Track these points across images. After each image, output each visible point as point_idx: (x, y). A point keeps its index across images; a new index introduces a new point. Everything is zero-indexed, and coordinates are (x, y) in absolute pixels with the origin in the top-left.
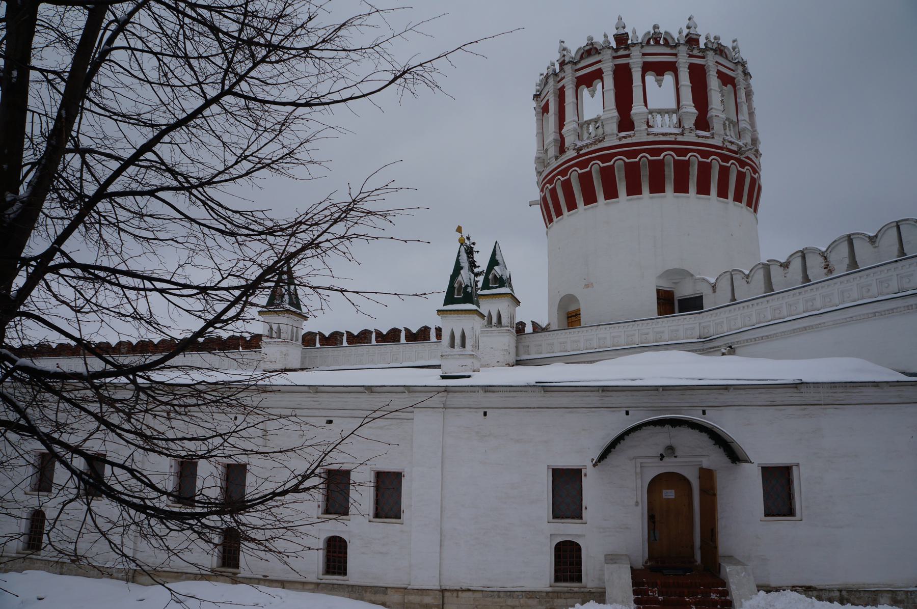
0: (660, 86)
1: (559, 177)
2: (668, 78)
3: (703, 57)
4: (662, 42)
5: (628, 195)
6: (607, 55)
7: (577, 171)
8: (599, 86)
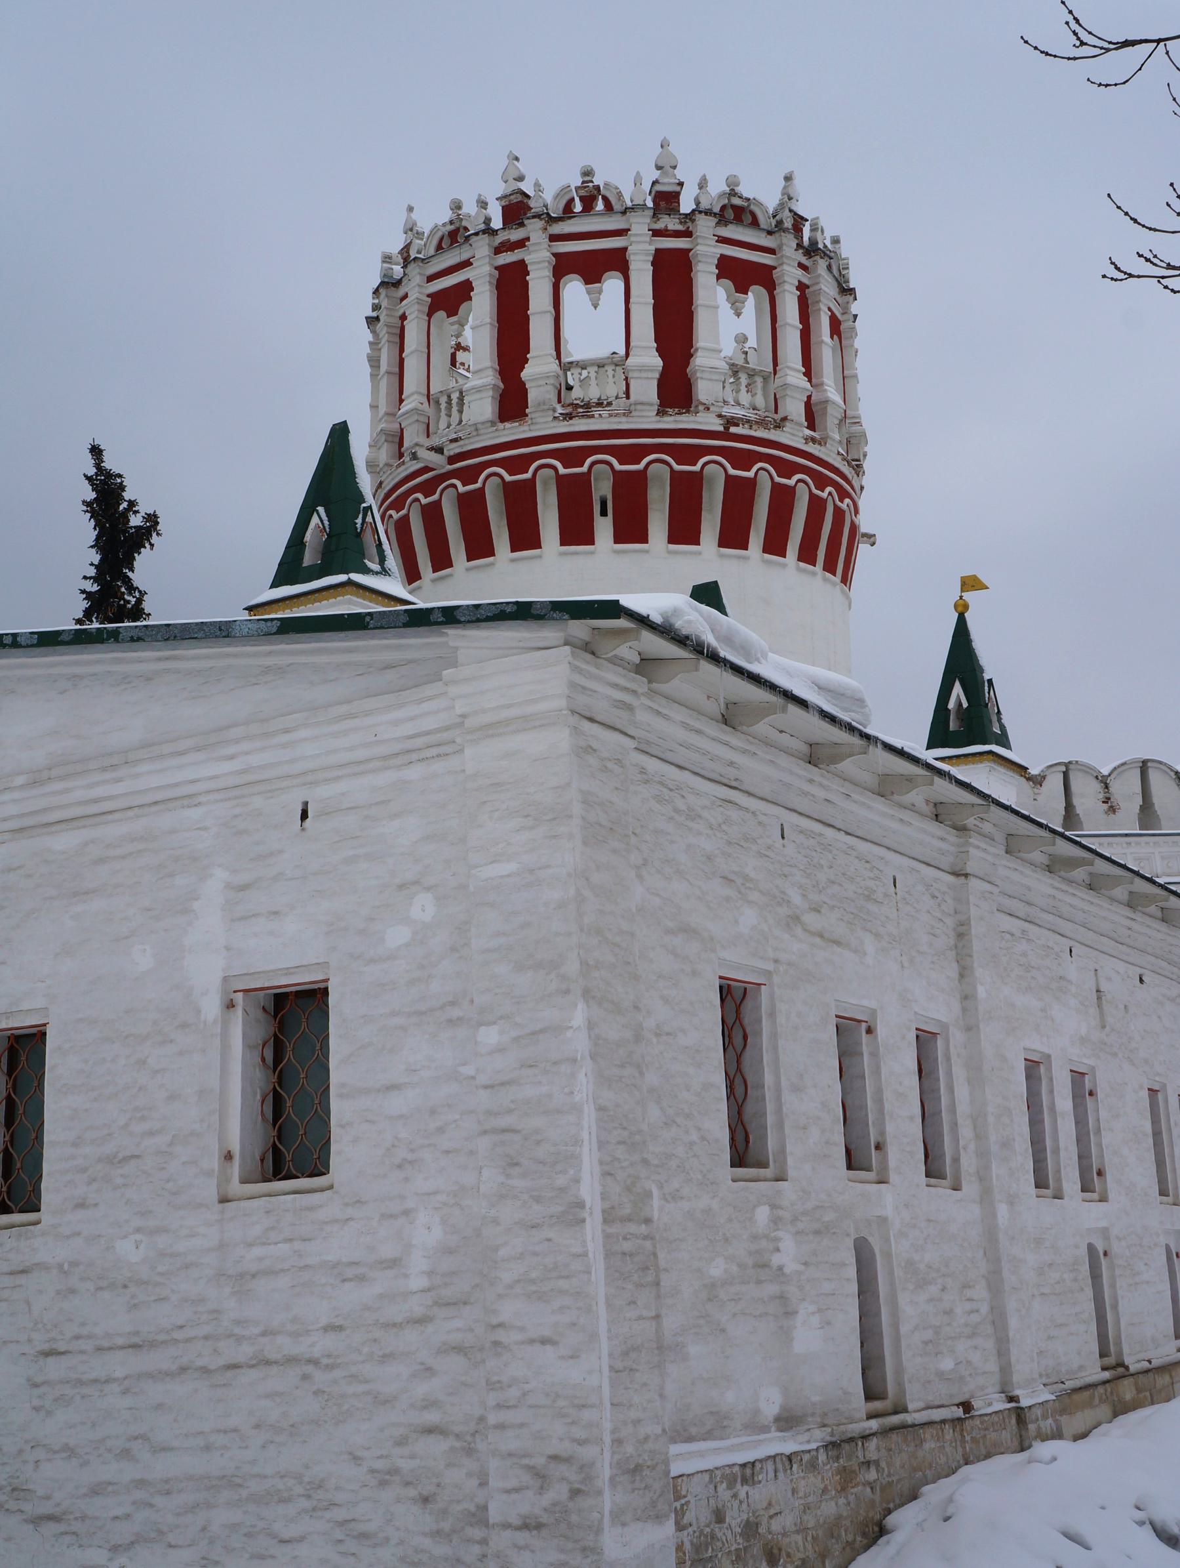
1: (419, 495)
2: (612, 285)
3: (688, 234)
7: (454, 486)
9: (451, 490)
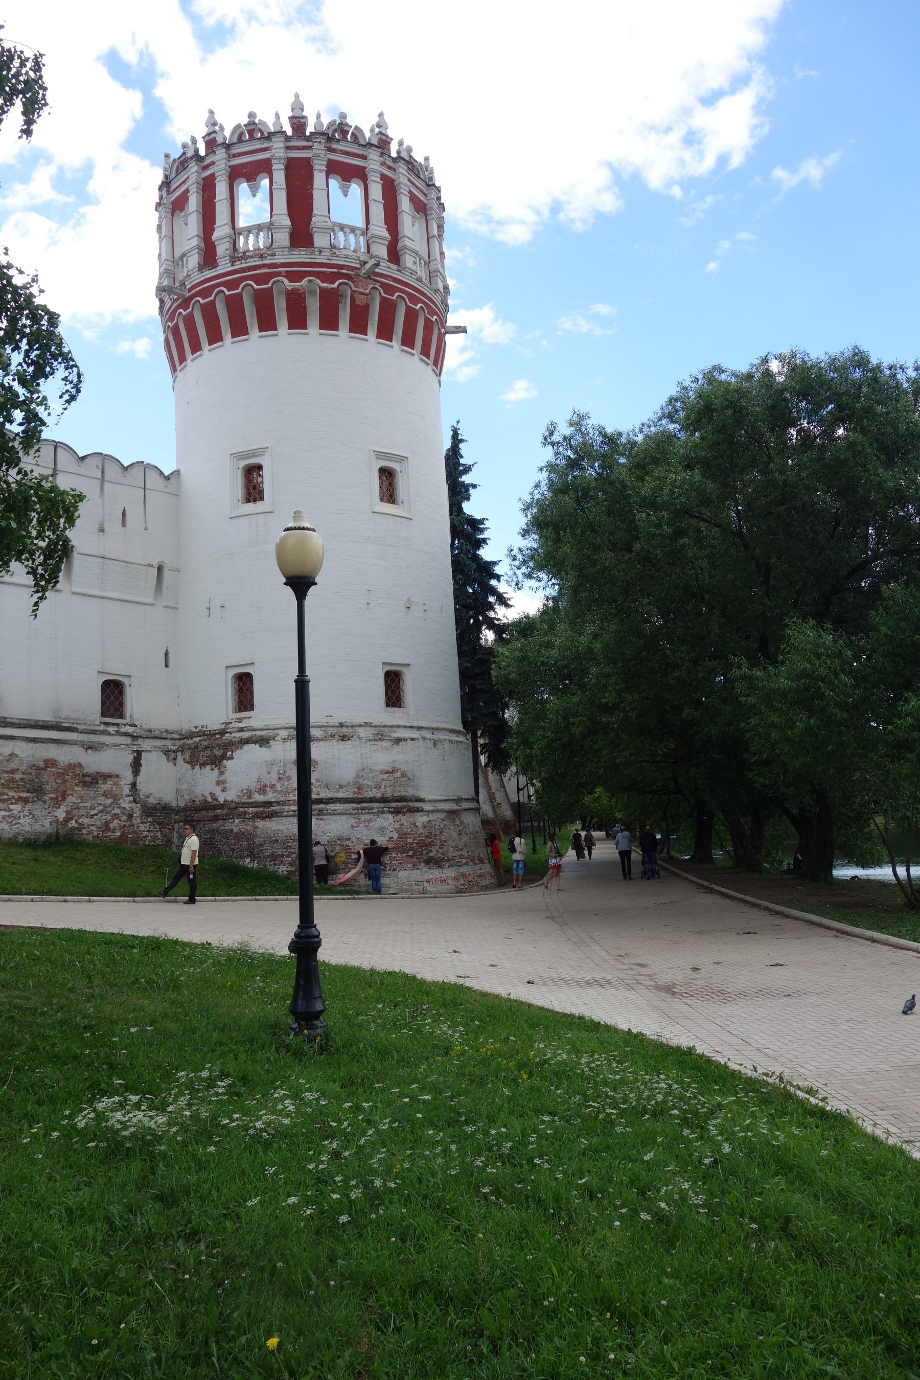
0: (346, 195)
4: (349, 137)
5: (289, 328)
6: (278, 145)
7: (223, 292)
8: (265, 182)
9: (222, 294)
